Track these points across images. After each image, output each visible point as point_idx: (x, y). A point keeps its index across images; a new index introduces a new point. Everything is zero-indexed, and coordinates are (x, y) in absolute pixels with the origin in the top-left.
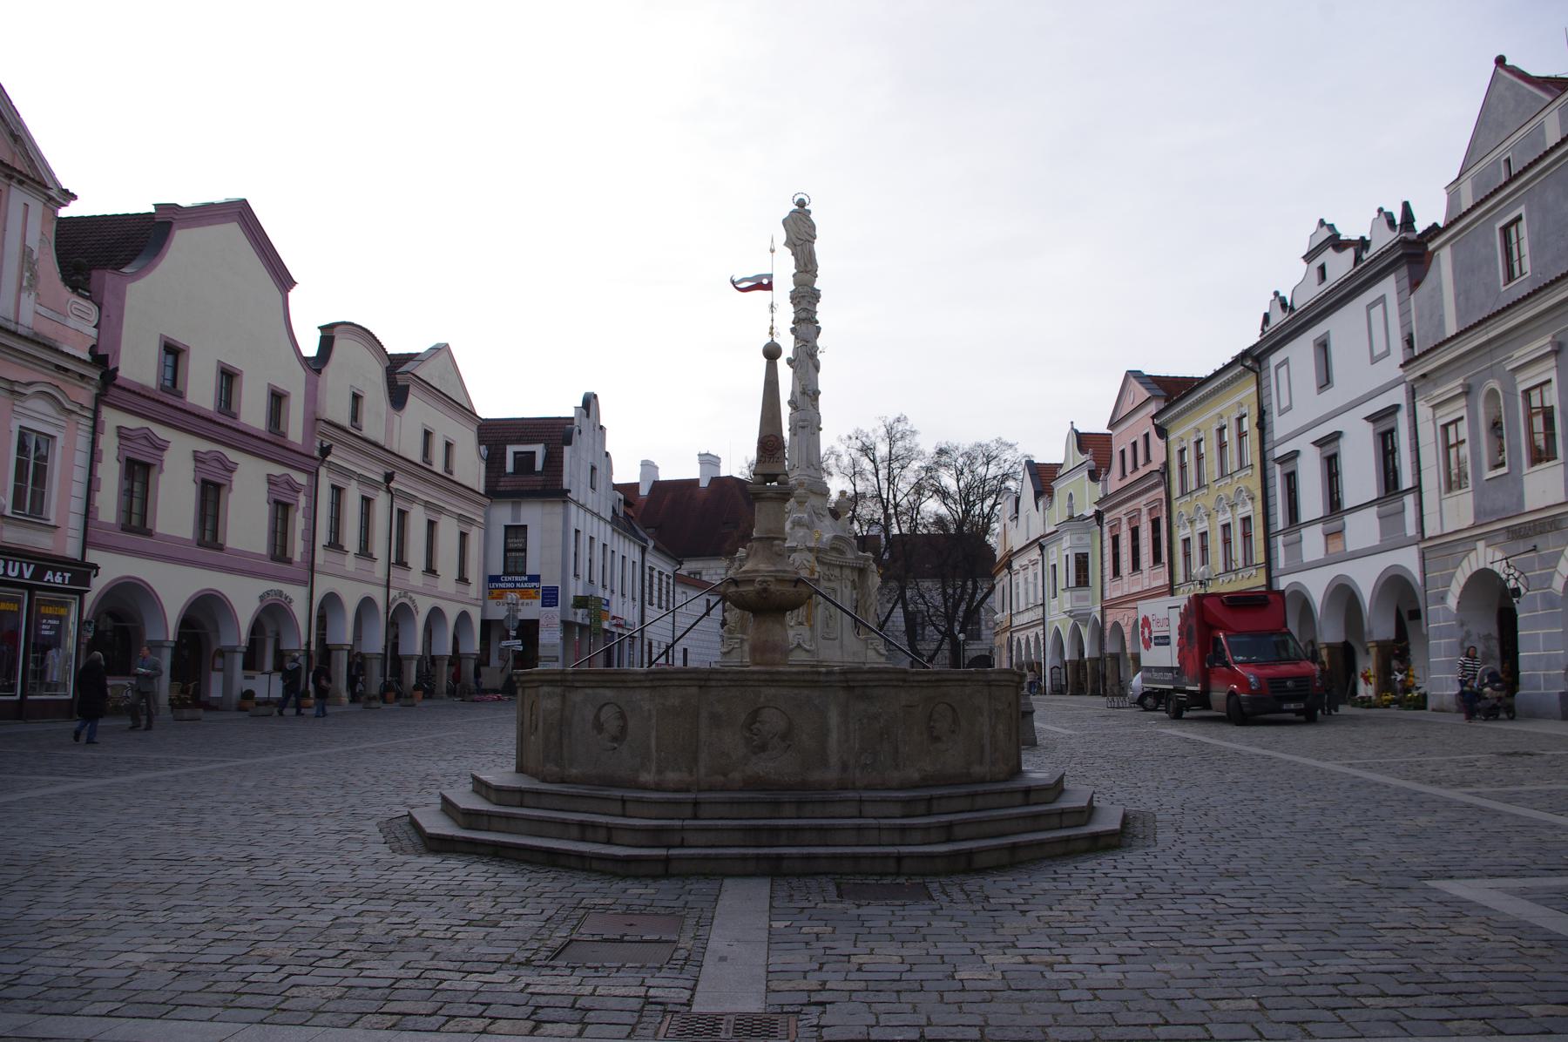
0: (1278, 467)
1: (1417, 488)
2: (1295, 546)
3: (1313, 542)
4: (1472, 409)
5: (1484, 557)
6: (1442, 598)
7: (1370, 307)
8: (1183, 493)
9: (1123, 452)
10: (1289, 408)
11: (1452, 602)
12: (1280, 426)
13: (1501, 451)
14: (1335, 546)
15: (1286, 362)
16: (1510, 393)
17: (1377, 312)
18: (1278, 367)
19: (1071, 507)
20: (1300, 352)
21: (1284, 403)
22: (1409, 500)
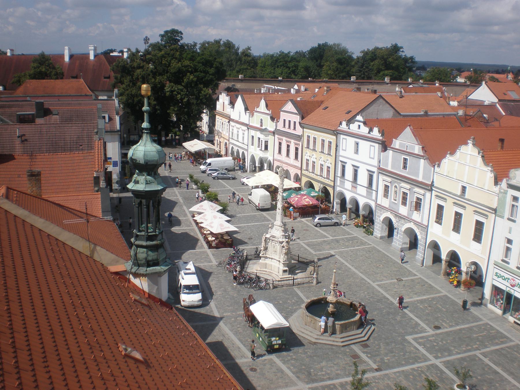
0: (340, 163)
1: (377, 192)
2: (342, 183)
3: (348, 185)
4: (392, 186)
5: (389, 215)
6: (379, 217)
7: (371, 146)
8: (308, 147)
9: (285, 120)
10: (345, 150)
11: (382, 218)
12: (341, 153)
13: (396, 197)
14: (354, 189)
15: (346, 139)
16: (400, 190)
17: (372, 148)
18: (343, 138)
19: (261, 122)
20: (351, 141)
21: (344, 148)
22: (374, 193)
